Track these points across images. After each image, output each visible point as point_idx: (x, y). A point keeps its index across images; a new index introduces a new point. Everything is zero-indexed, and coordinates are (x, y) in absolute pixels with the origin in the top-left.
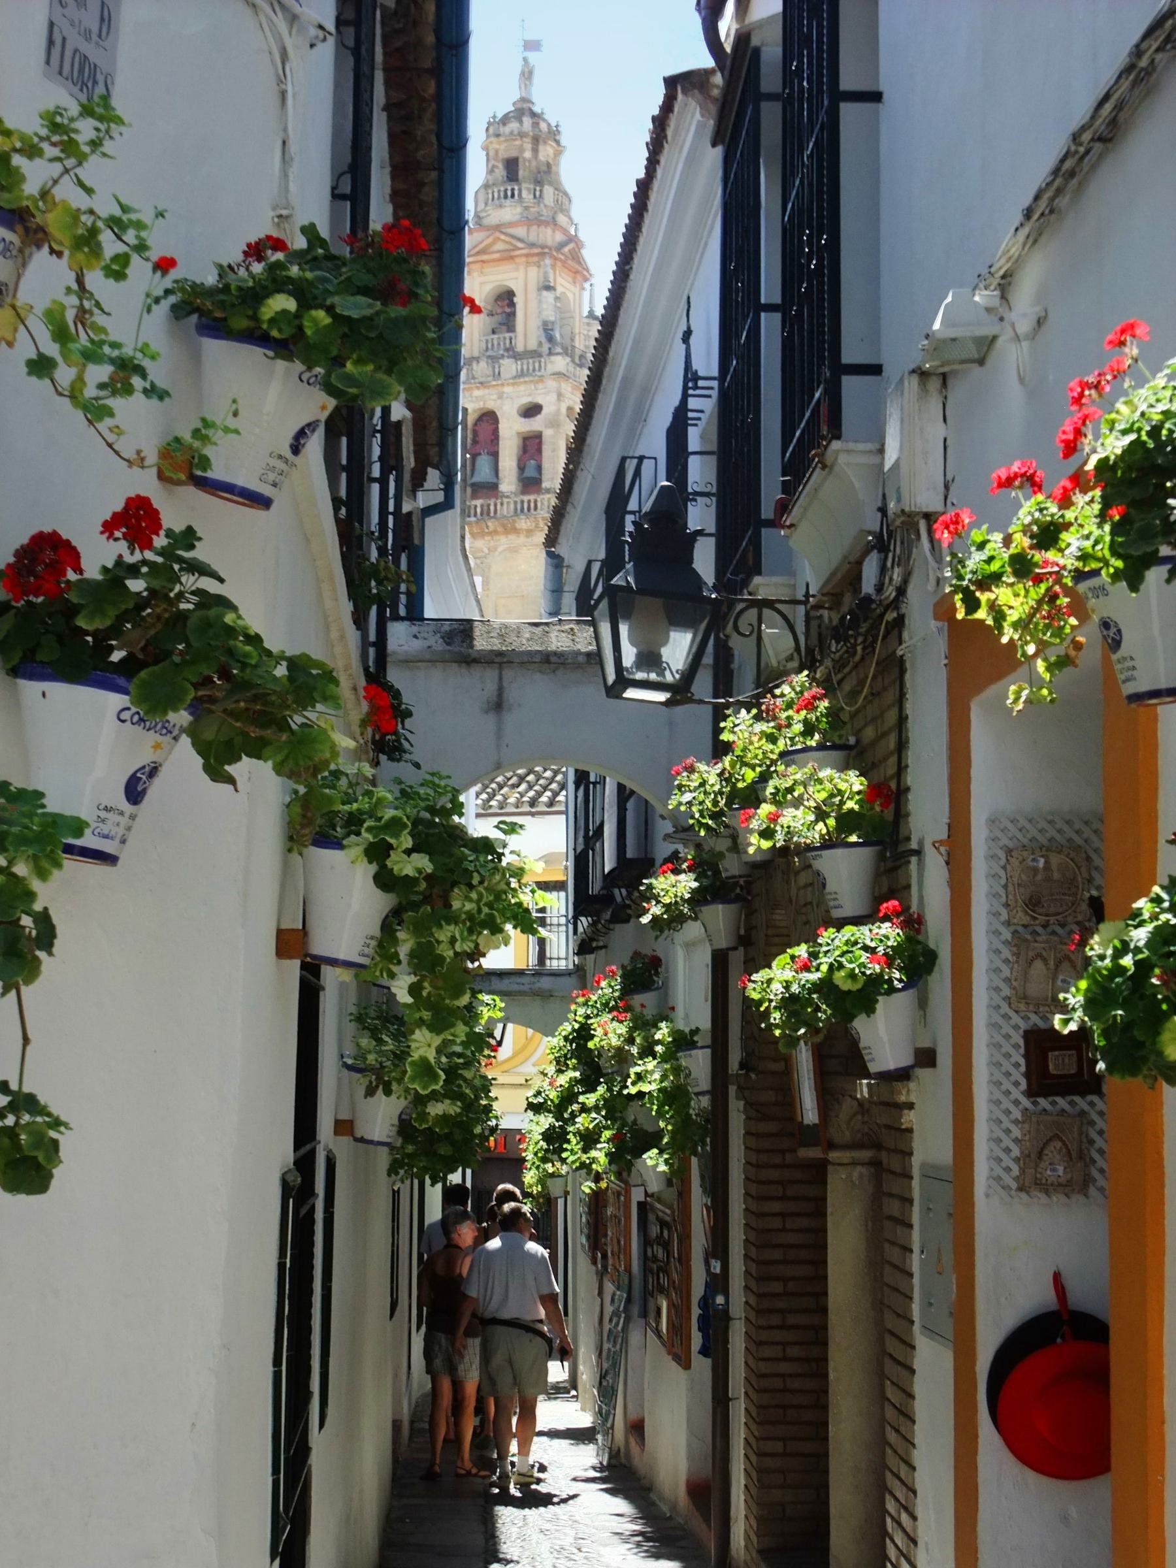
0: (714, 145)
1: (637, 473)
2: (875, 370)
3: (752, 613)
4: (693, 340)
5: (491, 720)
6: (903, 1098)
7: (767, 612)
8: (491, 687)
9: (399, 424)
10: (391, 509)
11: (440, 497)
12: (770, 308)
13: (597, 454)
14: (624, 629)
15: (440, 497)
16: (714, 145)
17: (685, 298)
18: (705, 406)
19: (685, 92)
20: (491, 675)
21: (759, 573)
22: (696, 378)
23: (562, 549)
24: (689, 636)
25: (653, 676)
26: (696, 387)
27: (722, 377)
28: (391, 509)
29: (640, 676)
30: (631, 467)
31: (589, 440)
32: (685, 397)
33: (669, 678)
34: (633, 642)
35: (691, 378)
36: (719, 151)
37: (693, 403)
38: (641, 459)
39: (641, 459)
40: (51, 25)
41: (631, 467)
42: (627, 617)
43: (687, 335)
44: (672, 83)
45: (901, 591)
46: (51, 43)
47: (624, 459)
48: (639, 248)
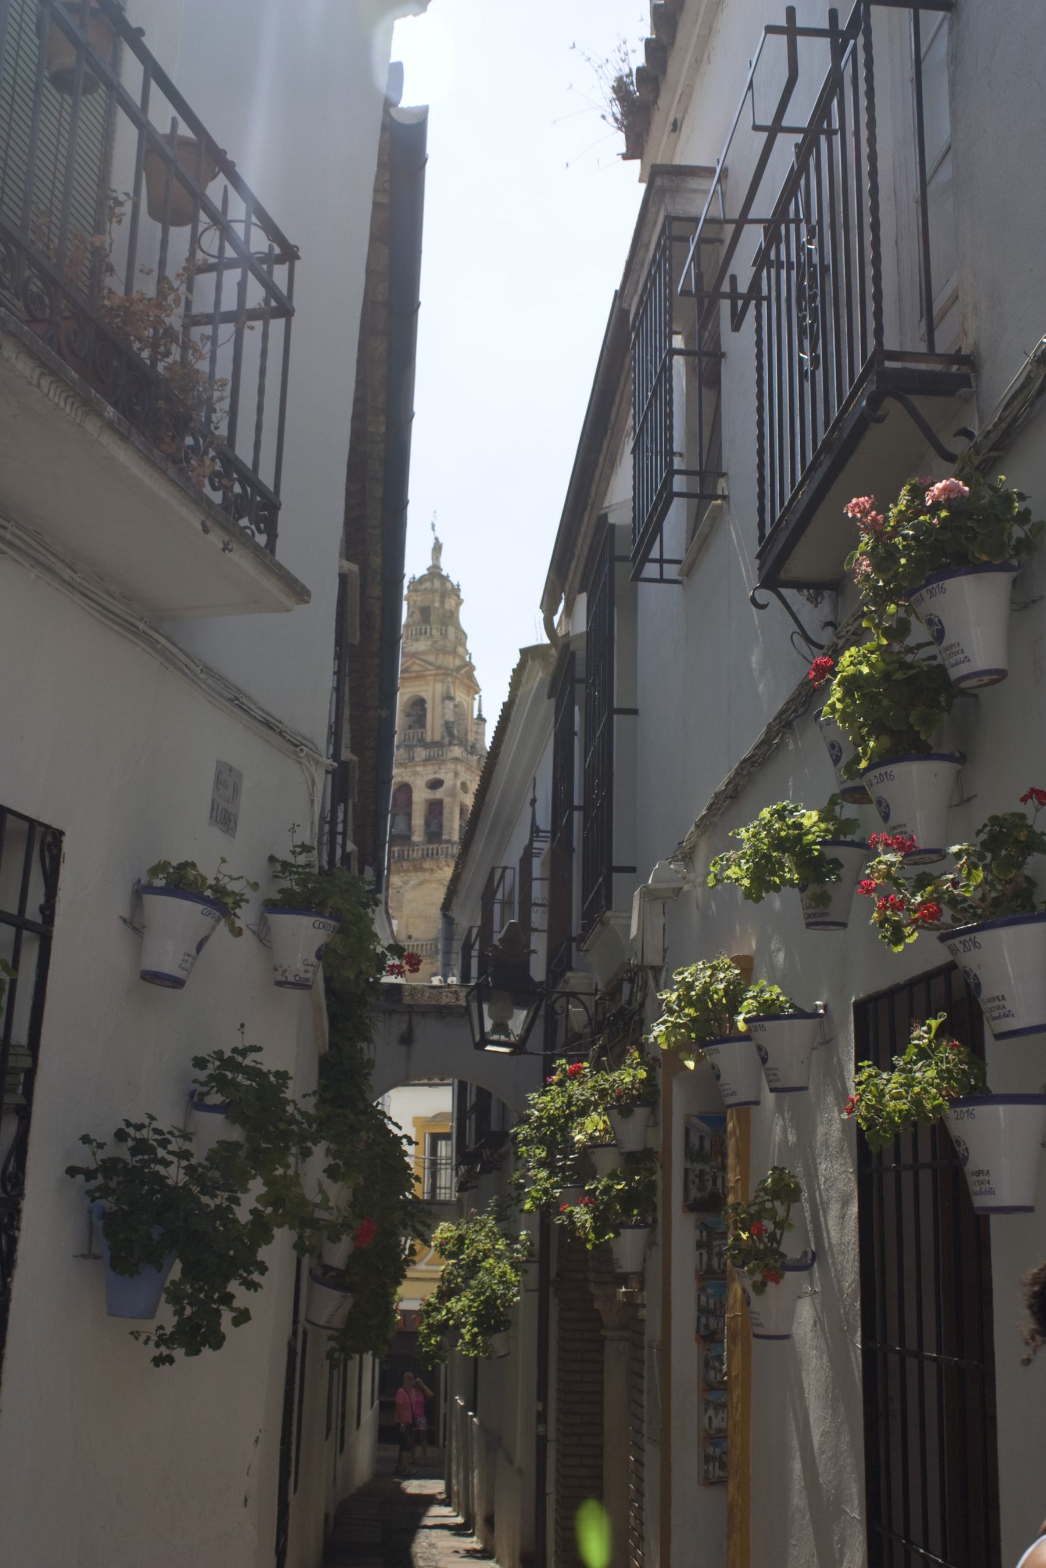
1: (502, 877)
2: (632, 870)
3: (564, 999)
4: (537, 805)
6: (639, 1301)
7: (572, 999)
9: (350, 853)
12: (578, 808)
14: (485, 1007)
16: (549, 698)
18: (543, 846)
19: (533, 660)
21: (571, 969)
22: (538, 831)
24: (525, 1012)
25: (503, 1038)
26: (538, 836)
27: (554, 831)
29: (495, 1037)
32: (531, 841)
33: (512, 1039)
34: (490, 1016)
35: (535, 830)
36: (553, 700)
37: (536, 845)
38: (505, 868)
39: (505, 868)
40: (213, 800)
42: (488, 1000)
43: (533, 802)
44: (524, 652)
45: (642, 1005)
46: (213, 809)
47: (493, 869)
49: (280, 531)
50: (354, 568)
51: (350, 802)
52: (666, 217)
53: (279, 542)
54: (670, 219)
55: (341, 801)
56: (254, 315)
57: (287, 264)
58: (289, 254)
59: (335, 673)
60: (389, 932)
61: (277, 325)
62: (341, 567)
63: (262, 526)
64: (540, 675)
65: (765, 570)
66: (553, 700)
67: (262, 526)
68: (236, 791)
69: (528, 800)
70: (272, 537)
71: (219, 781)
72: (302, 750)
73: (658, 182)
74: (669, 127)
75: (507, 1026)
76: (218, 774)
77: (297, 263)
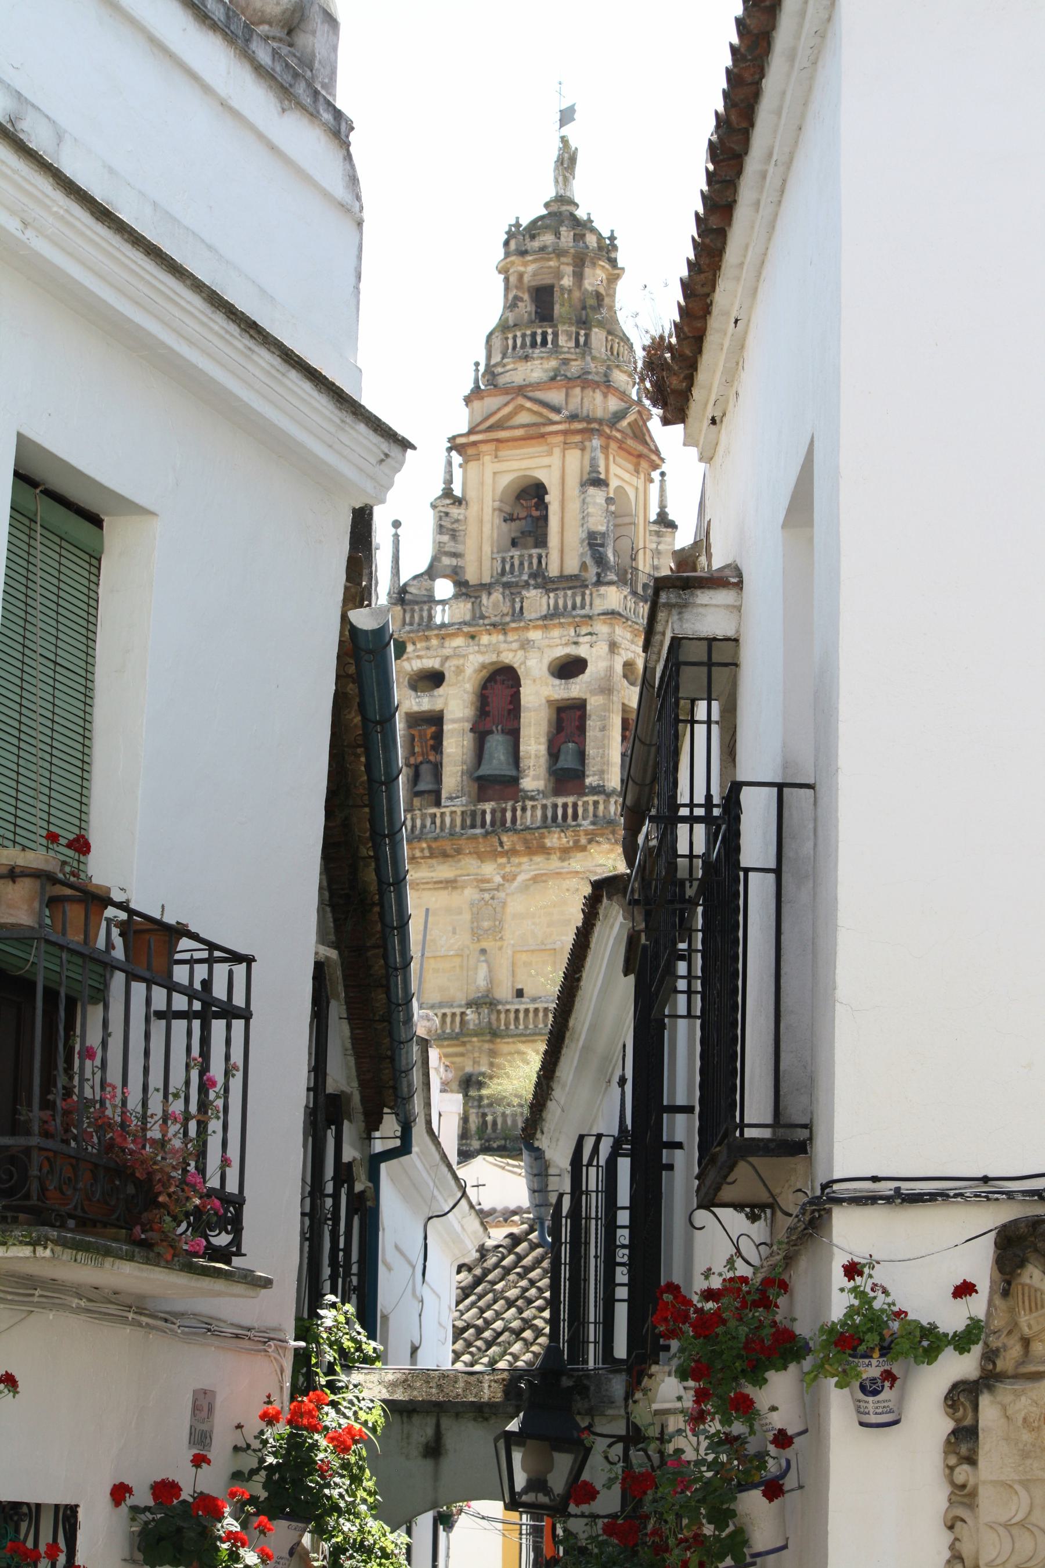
0: (625, 975)
5: (429, 1463)
8: (430, 1431)
9: (350, 1164)
10: (342, 1246)
11: (397, 1143)
13: (583, 1037)
15: (397, 1143)
16: (626, 974)
17: (620, 1046)
20: (431, 1421)
23: (536, 1144)
28: (342, 1246)
31: (571, 1023)
36: (632, 978)
38: (599, 1137)
39: (599, 1137)
46: (191, 1434)
47: (581, 1138)
48: (592, 945)
49: (245, 1223)
50: (333, 954)
51: (346, 1123)
52: (673, 639)
54: (676, 642)
56: (217, 1016)
57: (245, 964)
59: (309, 1089)
60: (437, 1157)
61: (238, 1025)
62: (316, 953)
63: (229, 1227)
64: (620, 919)
65: (704, 1190)
66: (632, 978)
67: (229, 1227)
68: (211, 1409)
69: (616, 1079)
71: (196, 1408)
72: (270, 1346)
73: (663, 598)
74: (707, 422)
75: (545, 1481)
76: (195, 1401)
77: (253, 964)
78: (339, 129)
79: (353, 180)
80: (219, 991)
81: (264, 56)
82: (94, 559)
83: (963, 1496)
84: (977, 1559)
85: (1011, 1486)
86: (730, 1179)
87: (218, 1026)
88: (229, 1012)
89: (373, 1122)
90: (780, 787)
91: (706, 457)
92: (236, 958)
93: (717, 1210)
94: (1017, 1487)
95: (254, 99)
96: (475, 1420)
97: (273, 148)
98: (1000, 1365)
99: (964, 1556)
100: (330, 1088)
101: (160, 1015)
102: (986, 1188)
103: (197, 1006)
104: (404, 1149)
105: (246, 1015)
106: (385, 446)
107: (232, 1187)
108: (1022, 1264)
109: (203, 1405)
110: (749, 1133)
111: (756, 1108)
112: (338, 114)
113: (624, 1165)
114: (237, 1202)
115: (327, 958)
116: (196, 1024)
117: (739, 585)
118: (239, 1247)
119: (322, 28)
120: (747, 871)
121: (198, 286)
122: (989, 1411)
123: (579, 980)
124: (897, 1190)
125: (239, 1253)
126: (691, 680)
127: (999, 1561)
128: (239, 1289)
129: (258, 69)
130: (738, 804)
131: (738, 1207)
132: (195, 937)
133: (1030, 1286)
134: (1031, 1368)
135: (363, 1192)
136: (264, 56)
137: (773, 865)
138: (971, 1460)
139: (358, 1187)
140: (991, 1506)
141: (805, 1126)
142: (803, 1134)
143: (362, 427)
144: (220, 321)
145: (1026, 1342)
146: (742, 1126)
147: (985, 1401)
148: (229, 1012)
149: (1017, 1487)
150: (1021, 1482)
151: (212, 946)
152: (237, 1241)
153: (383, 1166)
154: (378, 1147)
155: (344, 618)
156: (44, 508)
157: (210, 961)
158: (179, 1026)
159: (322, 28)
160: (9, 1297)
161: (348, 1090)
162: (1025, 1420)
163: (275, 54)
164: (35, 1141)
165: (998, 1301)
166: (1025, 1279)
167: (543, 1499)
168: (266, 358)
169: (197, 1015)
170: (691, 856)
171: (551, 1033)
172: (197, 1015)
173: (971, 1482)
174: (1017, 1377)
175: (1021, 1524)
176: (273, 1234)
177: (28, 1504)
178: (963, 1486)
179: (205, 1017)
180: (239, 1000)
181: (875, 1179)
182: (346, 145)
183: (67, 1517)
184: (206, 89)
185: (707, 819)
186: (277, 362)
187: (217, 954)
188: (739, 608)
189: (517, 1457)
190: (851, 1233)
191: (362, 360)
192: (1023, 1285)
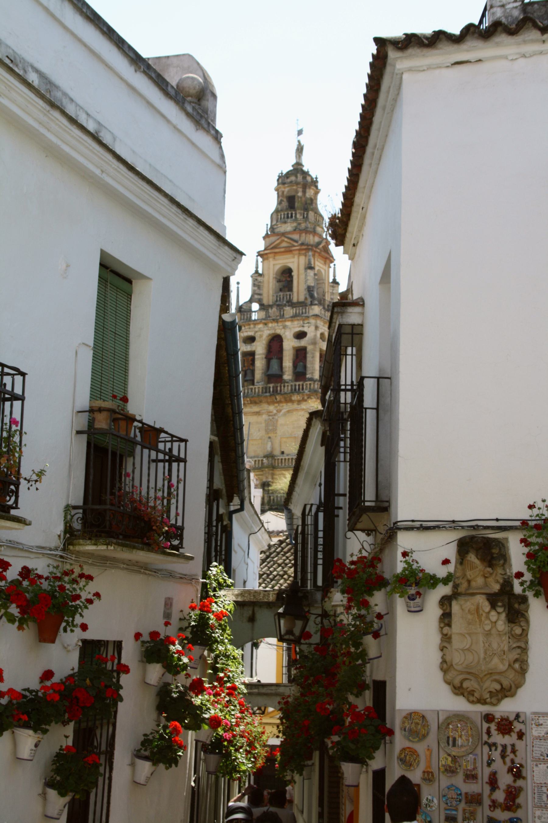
8: (250, 612)
9: (222, 515)
10: (219, 544)
11: (239, 507)
15: (239, 507)
16: (322, 445)
17: (319, 472)
23: (289, 507)
28: (219, 544)
30: (308, 508)
31: (302, 463)
36: (324, 448)
38: (312, 505)
39: (312, 505)
41: (308, 508)
47: (305, 506)
48: (310, 435)
50: (216, 439)
51: (221, 500)
53: (184, 541)
54: (340, 326)
55: (214, 500)
56: (174, 461)
58: (186, 441)
59: (207, 488)
60: (253, 512)
61: (182, 464)
64: (320, 426)
68: (171, 605)
69: (318, 484)
70: (181, 539)
71: (166, 604)
73: (336, 310)
74: (351, 245)
78: (217, 137)
79: (222, 156)
80: (175, 452)
81: (189, 109)
82: (129, 296)
83: (446, 639)
84: (452, 662)
85: (464, 635)
86: (360, 521)
87: (175, 465)
88: (179, 460)
89: (230, 499)
90: (378, 378)
91: (351, 258)
92: (181, 440)
93: (355, 532)
94: (467, 636)
95: (186, 125)
96: (267, 608)
97: (193, 144)
98: (460, 590)
99: (447, 661)
100: (215, 487)
101: (154, 461)
102: (453, 525)
103: (167, 457)
104: (242, 509)
105: (184, 461)
106: (235, 254)
107: (179, 523)
108: (467, 552)
109: (168, 603)
110: (367, 504)
111: (369, 495)
112: (217, 132)
113: (321, 515)
114: (182, 529)
115: (214, 440)
116: (167, 464)
117: (363, 305)
118: (182, 545)
119: (211, 99)
120: (366, 409)
121: (166, 195)
122: (456, 607)
123: (305, 448)
124: (421, 525)
125: (182, 548)
126: (345, 339)
127: (460, 663)
128: (182, 560)
129: (188, 114)
130: (363, 385)
131: (363, 530)
132: (166, 433)
133: (470, 561)
134: (471, 591)
135: (226, 525)
136: (189, 109)
137: (375, 406)
138: (449, 625)
139: (225, 523)
140: (457, 643)
141: (387, 502)
142: (386, 504)
143: (226, 248)
144: (174, 209)
145: (469, 582)
146: (364, 501)
147: (454, 603)
148: (179, 460)
149: (467, 636)
150: (468, 634)
151: (172, 436)
152: (181, 543)
153: (234, 516)
154: (232, 508)
155: (220, 317)
156: (111, 277)
157: (172, 441)
158: (161, 465)
159: (211, 99)
160: (98, 564)
161: (221, 488)
162: (469, 611)
163: (194, 108)
164: (108, 507)
165: (459, 566)
166: (469, 558)
167: (292, 637)
168: (191, 222)
169: (167, 461)
170: (345, 403)
171: (294, 467)
172: (167, 461)
173: (449, 633)
174: (466, 594)
175: (468, 649)
176: (194, 541)
177: (104, 641)
178: (446, 635)
179: (170, 462)
180: (182, 455)
181: (413, 521)
182: (219, 143)
183: (118, 645)
184: (168, 121)
185: (352, 390)
186: (195, 223)
187: (174, 439)
188: (363, 314)
189: (282, 622)
190: (405, 541)
191: (226, 223)
192: (468, 560)
